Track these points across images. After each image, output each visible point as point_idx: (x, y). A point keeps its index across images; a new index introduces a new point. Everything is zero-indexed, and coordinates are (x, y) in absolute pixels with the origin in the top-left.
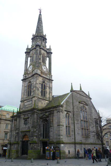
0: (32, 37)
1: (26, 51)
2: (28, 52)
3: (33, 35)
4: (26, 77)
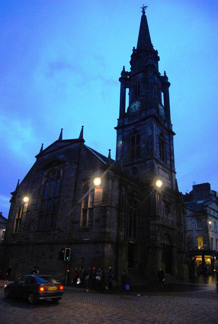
0: (131, 52)
1: (120, 76)
2: (125, 79)
3: (134, 50)
4: (123, 123)
